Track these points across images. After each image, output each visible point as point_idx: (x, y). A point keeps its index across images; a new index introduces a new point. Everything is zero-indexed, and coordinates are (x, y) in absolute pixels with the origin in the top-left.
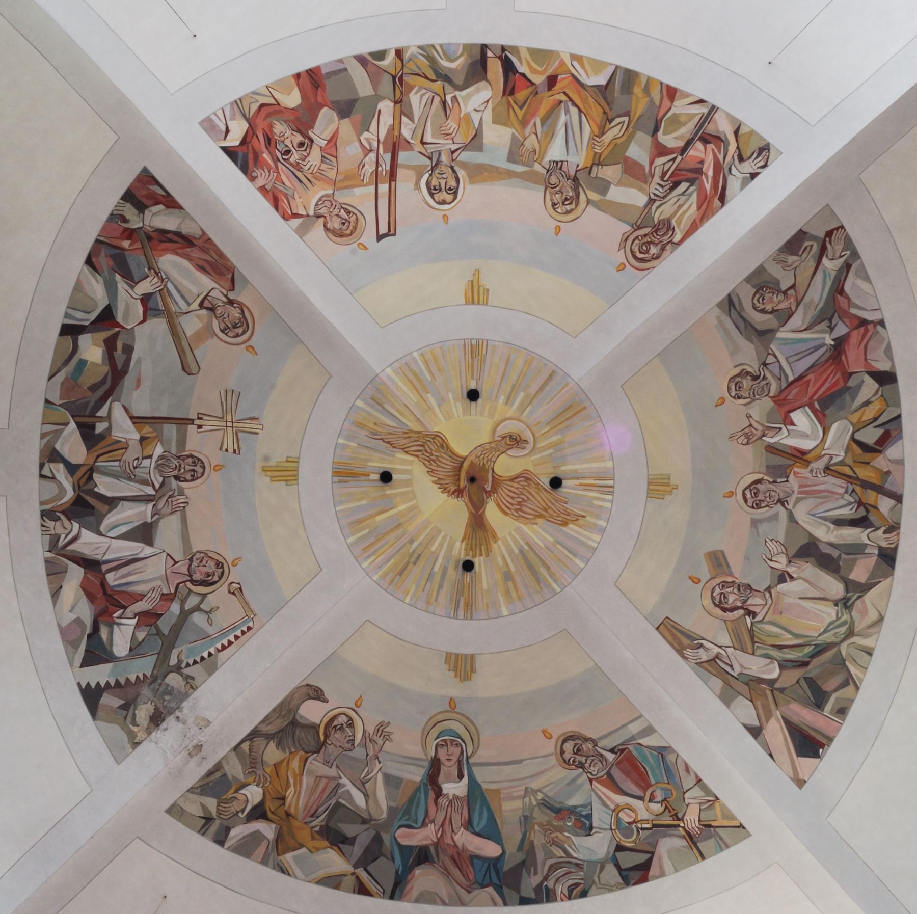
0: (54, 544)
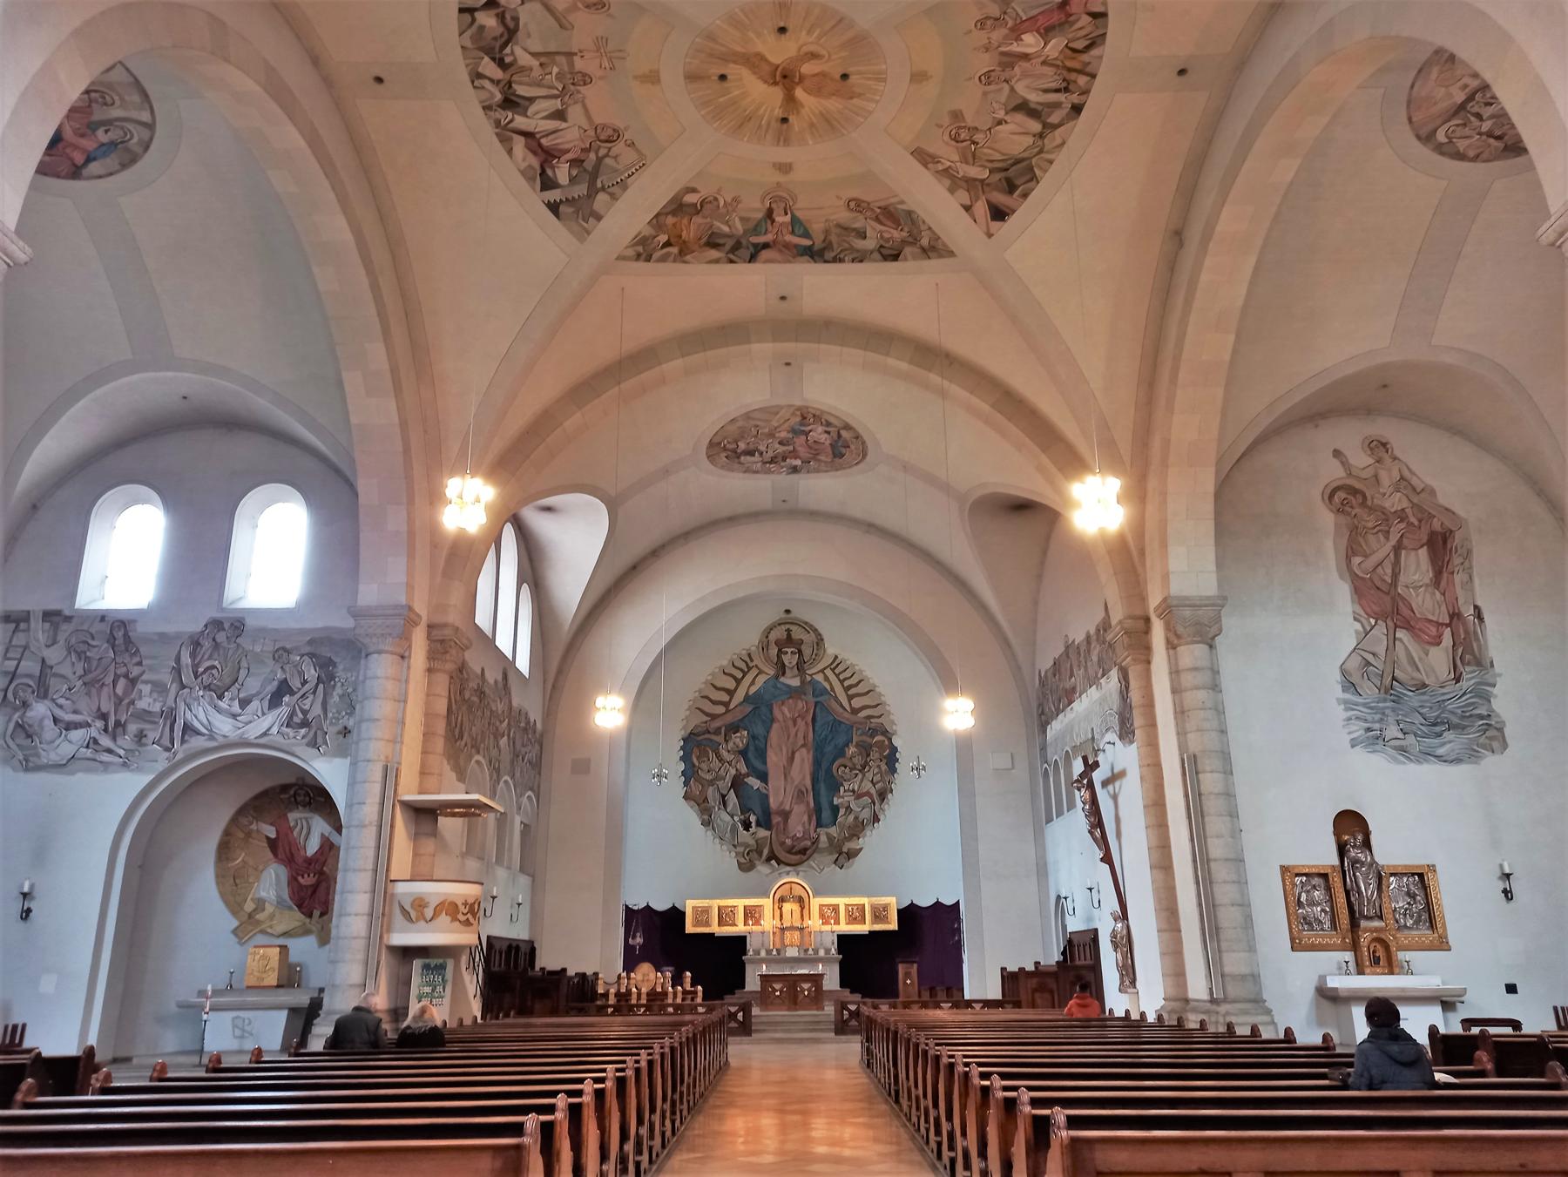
0: (497, 123)
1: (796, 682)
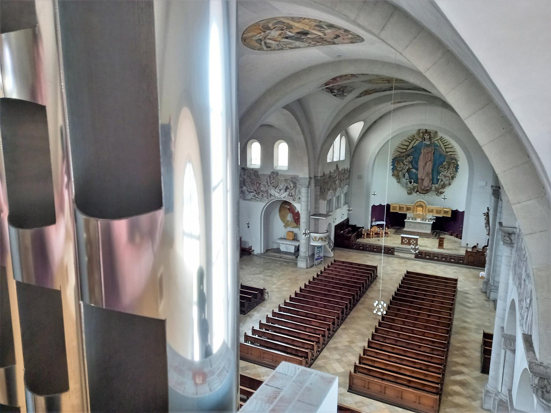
1: (429, 143)
